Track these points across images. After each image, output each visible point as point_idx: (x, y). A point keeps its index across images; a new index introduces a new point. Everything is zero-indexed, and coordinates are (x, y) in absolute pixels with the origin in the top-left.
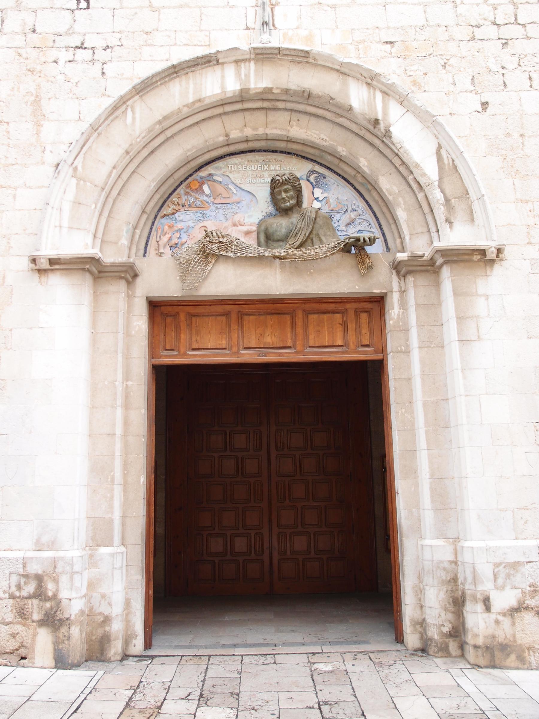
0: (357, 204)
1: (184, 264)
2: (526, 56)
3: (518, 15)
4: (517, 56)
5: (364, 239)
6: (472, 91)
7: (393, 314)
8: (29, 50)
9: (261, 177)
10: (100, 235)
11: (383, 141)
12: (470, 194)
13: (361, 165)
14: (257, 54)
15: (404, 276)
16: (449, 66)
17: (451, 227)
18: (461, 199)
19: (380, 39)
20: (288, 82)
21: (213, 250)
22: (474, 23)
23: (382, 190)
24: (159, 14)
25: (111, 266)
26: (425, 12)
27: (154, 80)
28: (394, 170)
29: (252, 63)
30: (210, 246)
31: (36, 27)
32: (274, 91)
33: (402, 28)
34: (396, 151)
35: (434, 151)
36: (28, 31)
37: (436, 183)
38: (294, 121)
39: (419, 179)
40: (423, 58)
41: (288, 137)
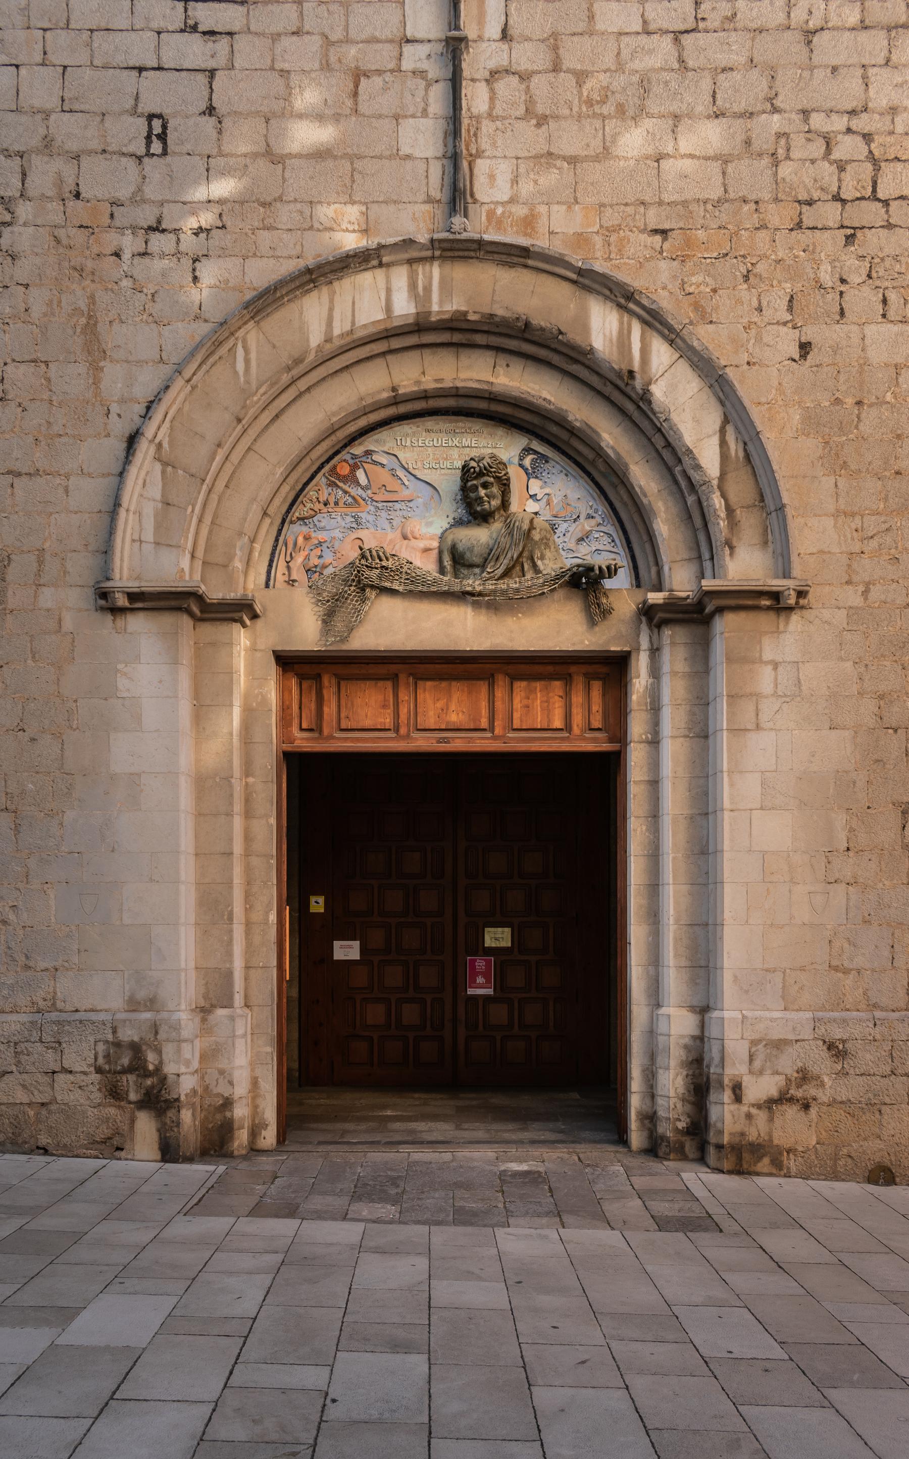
0: (595, 506)
1: (328, 601)
2: (882, 259)
3: (879, 181)
4: (868, 259)
5: (600, 568)
6: (787, 322)
7: (637, 685)
8: (73, 232)
9: (446, 459)
10: (200, 553)
11: (639, 407)
12: (766, 501)
13: (603, 444)
14: (444, 250)
15: (659, 626)
16: (755, 276)
17: (731, 554)
18: (750, 509)
19: (645, 224)
20: (493, 301)
21: (370, 577)
22: (803, 196)
23: (633, 488)
24: (284, 169)
25: (219, 604)
26: (724, 173)
27: (278, 294)
28: (654, 454)
29: (436, 264)
30: (367, 572)
31: (80, 187)
32: (469, 318)
33: (685, 203)
34: (659, 425)
35: (717, 426)
36: (67, 195)
37: (715, 483)
38: (501, 366)
39: (691, 473)
40: (713, 260)
41: (490, 393)
